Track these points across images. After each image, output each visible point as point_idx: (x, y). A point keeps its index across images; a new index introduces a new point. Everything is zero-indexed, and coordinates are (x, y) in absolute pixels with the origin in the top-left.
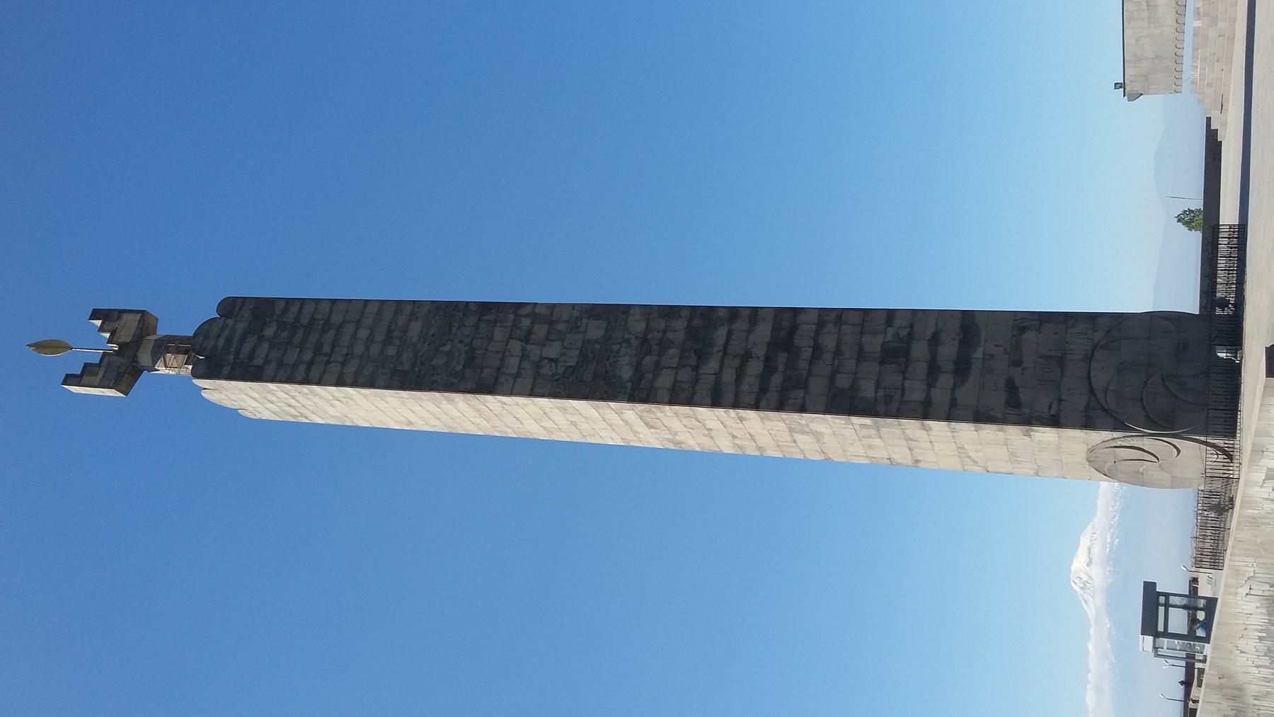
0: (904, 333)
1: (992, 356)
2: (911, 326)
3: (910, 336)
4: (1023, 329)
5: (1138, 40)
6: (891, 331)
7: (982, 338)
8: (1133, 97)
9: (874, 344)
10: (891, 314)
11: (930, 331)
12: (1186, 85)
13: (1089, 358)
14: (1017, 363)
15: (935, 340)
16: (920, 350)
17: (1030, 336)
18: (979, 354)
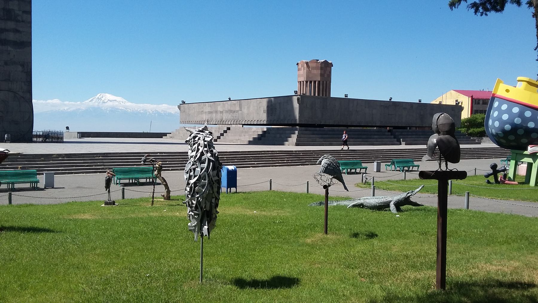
0: (19, 18)
1: (9, 54)
2: (23, 21)
3: (18, 21)
4: (23, 65)
5: (194, 108)
6: (20, 13)
7: (18, 50)
8: (179, 107)
9: (14, 6)
10: (29, 13)
11: (21, 29)
12: (184, 125)
13: (10, 90)
14: (6, 63)
15: (16, 31)
16: (11, 25)
17: (20, 68)
18: (10, 48)
